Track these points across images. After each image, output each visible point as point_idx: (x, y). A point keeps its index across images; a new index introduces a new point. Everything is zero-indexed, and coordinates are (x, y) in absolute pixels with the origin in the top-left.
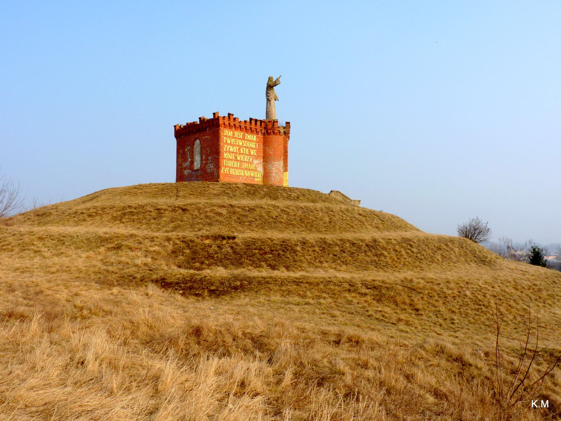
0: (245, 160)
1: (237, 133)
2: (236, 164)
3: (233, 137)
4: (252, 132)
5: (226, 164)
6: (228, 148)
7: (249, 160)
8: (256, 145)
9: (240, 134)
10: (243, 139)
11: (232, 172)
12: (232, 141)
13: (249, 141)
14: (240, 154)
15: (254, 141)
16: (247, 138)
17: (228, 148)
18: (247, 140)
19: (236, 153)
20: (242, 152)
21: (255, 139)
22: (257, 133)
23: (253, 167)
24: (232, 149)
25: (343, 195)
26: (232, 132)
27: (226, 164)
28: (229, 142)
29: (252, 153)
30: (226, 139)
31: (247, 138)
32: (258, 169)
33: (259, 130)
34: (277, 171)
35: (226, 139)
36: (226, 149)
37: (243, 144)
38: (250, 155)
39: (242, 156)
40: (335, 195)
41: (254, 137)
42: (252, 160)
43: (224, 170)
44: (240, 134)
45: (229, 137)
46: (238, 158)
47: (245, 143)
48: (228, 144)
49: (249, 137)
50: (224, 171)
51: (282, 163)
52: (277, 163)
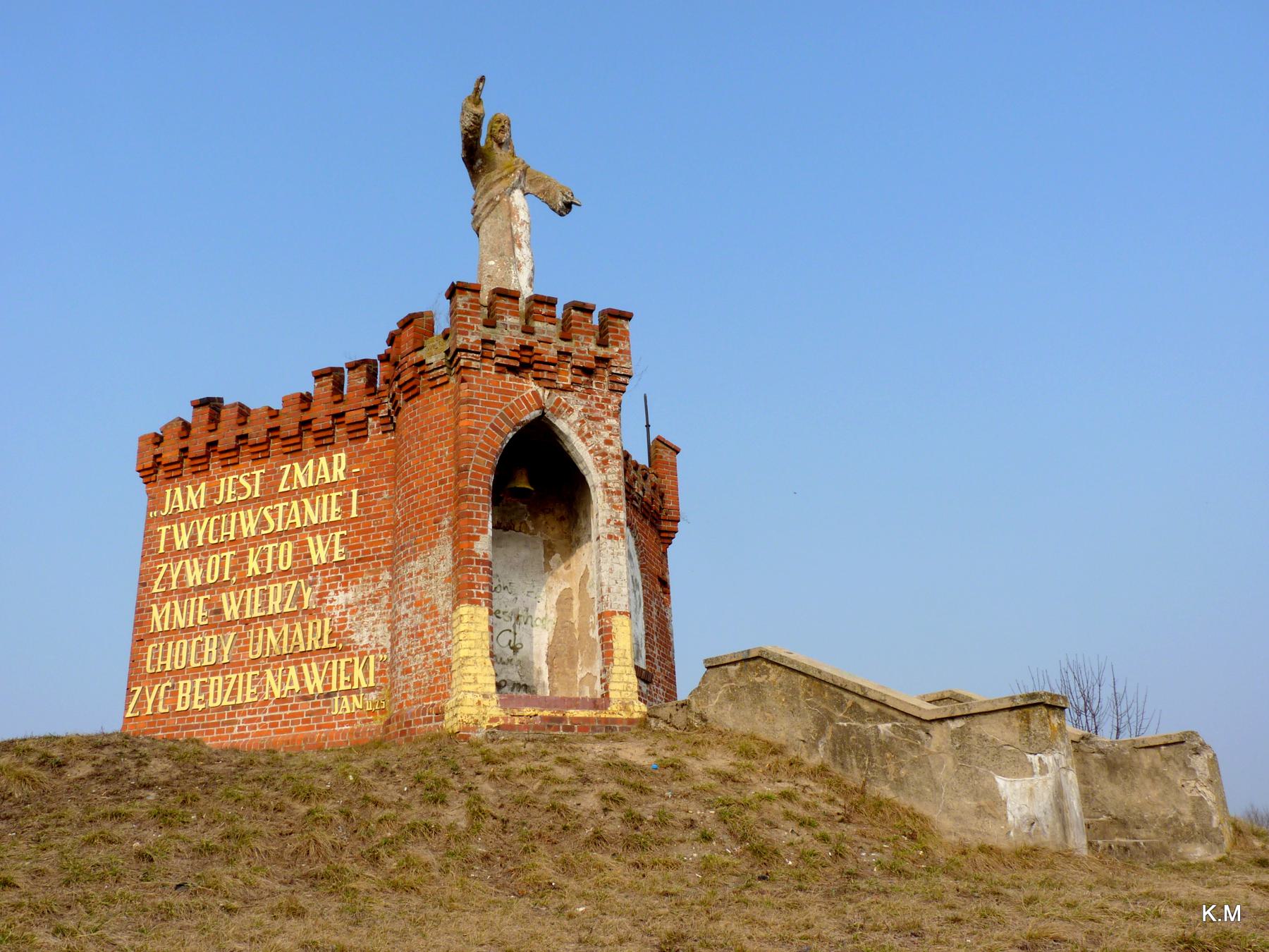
0: (274, 607)
1: (227, 486)
2: (215, 648)
3: (210, 509)
4: (325, 441)
5: (154, 662)
6: (175, 577)
7: (299, 599)
8: (344, 502)
9: (251, 479)
10: (269, 495)
11: (189, 696)
12: (201, 533)
13: (306, 492)
14: (244, 582)
15: (332, 486)
16: (290, 481)
17: (175, 577)
18: (288, 495)
19: (221, 585)
20: (253, 566)
21: (339, 474)
22: (358, 432)
23: (316, 634)
24: (198, 573)
25: (818, 681)
26: (203, 486)
27: (154, 662)
28: (182, 542)
29: (318, 553)
30: (170, 534)
31: (290, 481)
32: (361, 637)
33: (361, 414)
34: (419, 619)
35: (170, 534)
36: (167, 580)
37: (263, 524)
38: (303, 569)
39: (253, 595)
40: (732, 697)
41: (335, 466)
42: (322, 596)
43: (142, 696)
44: (251, 479)
45: (191, 515)
46: (231, 611)
47: (274, 513)
48: (177, 555)
49: (301, 473)
50: (141, 704)
51: (442, 557)
52: (418, 565)
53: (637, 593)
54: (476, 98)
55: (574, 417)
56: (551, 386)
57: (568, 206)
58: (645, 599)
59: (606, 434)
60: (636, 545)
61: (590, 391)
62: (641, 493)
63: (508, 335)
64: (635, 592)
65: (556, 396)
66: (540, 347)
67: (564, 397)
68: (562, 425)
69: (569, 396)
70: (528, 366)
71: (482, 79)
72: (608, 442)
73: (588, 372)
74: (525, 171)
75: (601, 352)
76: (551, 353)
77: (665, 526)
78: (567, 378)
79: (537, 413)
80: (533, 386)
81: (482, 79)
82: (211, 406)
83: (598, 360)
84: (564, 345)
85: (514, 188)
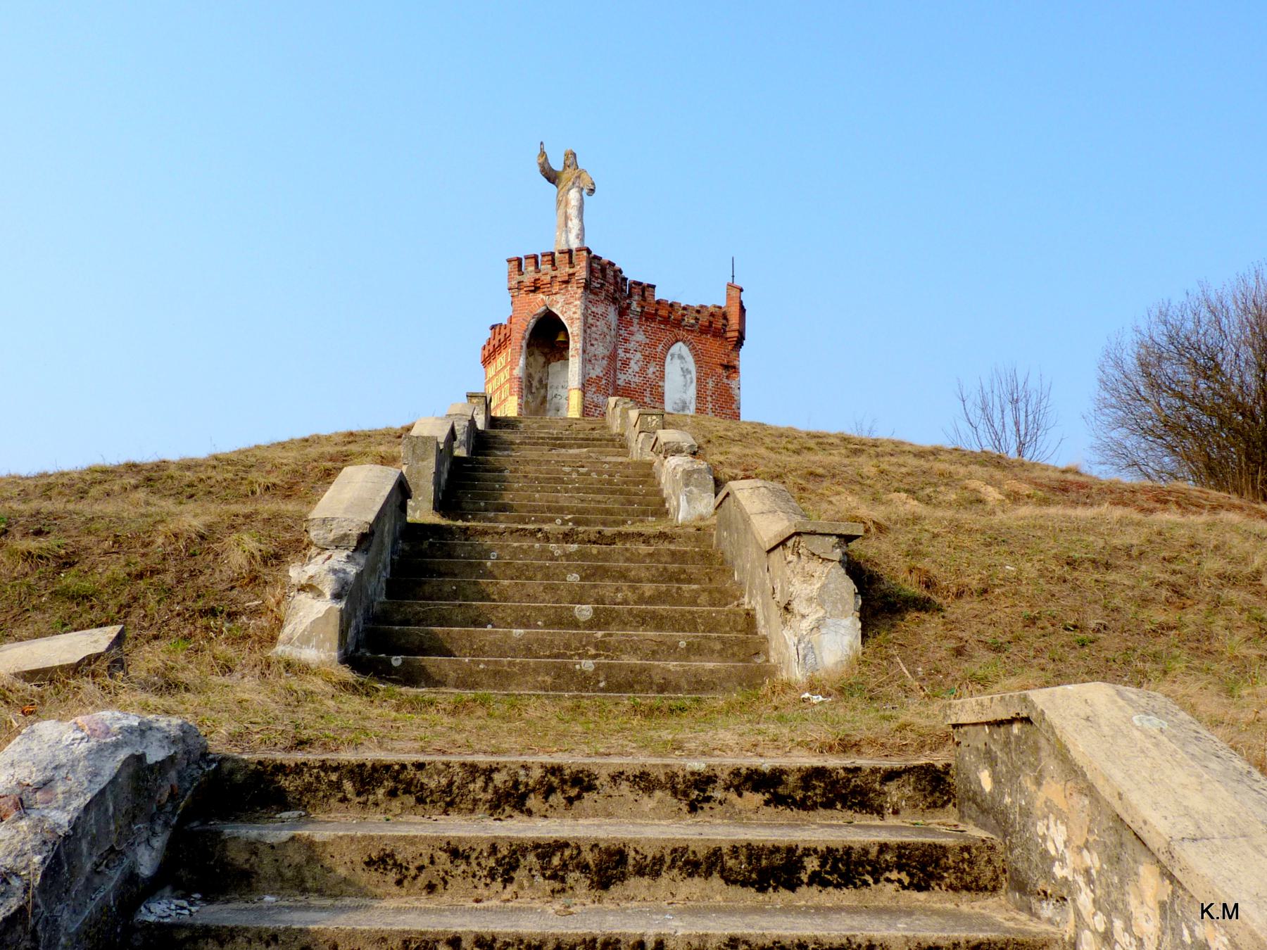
53: (688, 376)
54: (543, 153)
55: (559, 305)
56: (550, 294)
57: (592, 191)
58: (698, 379)
59: (574, 309)
60: (690, 350)
61: (567, 291)
62: (693, 321)
63: (529, 275)
64: (685, 376)
65: (551, 297)
66: (542, 278)
67: (554, 297)
68: (554, 310)
69: (558, 296)
70: (539, 288)
71: (542, 143)
72: (575, 313)
73: (567, 282)
74: (579, 177)
75: (571, 271)
76: (548, 279)
77: (729, 335)
78: (556, 288)
79: (544, 308)
80: (541, 296)
81: (542, 143)
82: (493, 327)
83: (569, 275)
84: (554, 273)
85: (569, 190)
